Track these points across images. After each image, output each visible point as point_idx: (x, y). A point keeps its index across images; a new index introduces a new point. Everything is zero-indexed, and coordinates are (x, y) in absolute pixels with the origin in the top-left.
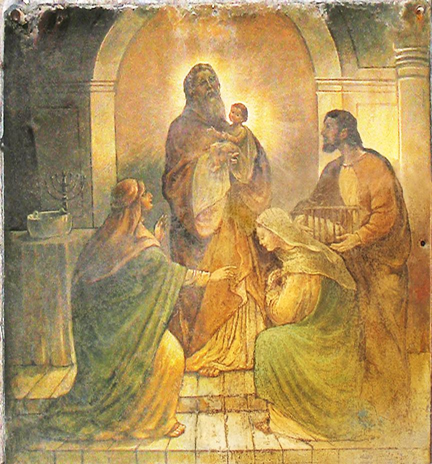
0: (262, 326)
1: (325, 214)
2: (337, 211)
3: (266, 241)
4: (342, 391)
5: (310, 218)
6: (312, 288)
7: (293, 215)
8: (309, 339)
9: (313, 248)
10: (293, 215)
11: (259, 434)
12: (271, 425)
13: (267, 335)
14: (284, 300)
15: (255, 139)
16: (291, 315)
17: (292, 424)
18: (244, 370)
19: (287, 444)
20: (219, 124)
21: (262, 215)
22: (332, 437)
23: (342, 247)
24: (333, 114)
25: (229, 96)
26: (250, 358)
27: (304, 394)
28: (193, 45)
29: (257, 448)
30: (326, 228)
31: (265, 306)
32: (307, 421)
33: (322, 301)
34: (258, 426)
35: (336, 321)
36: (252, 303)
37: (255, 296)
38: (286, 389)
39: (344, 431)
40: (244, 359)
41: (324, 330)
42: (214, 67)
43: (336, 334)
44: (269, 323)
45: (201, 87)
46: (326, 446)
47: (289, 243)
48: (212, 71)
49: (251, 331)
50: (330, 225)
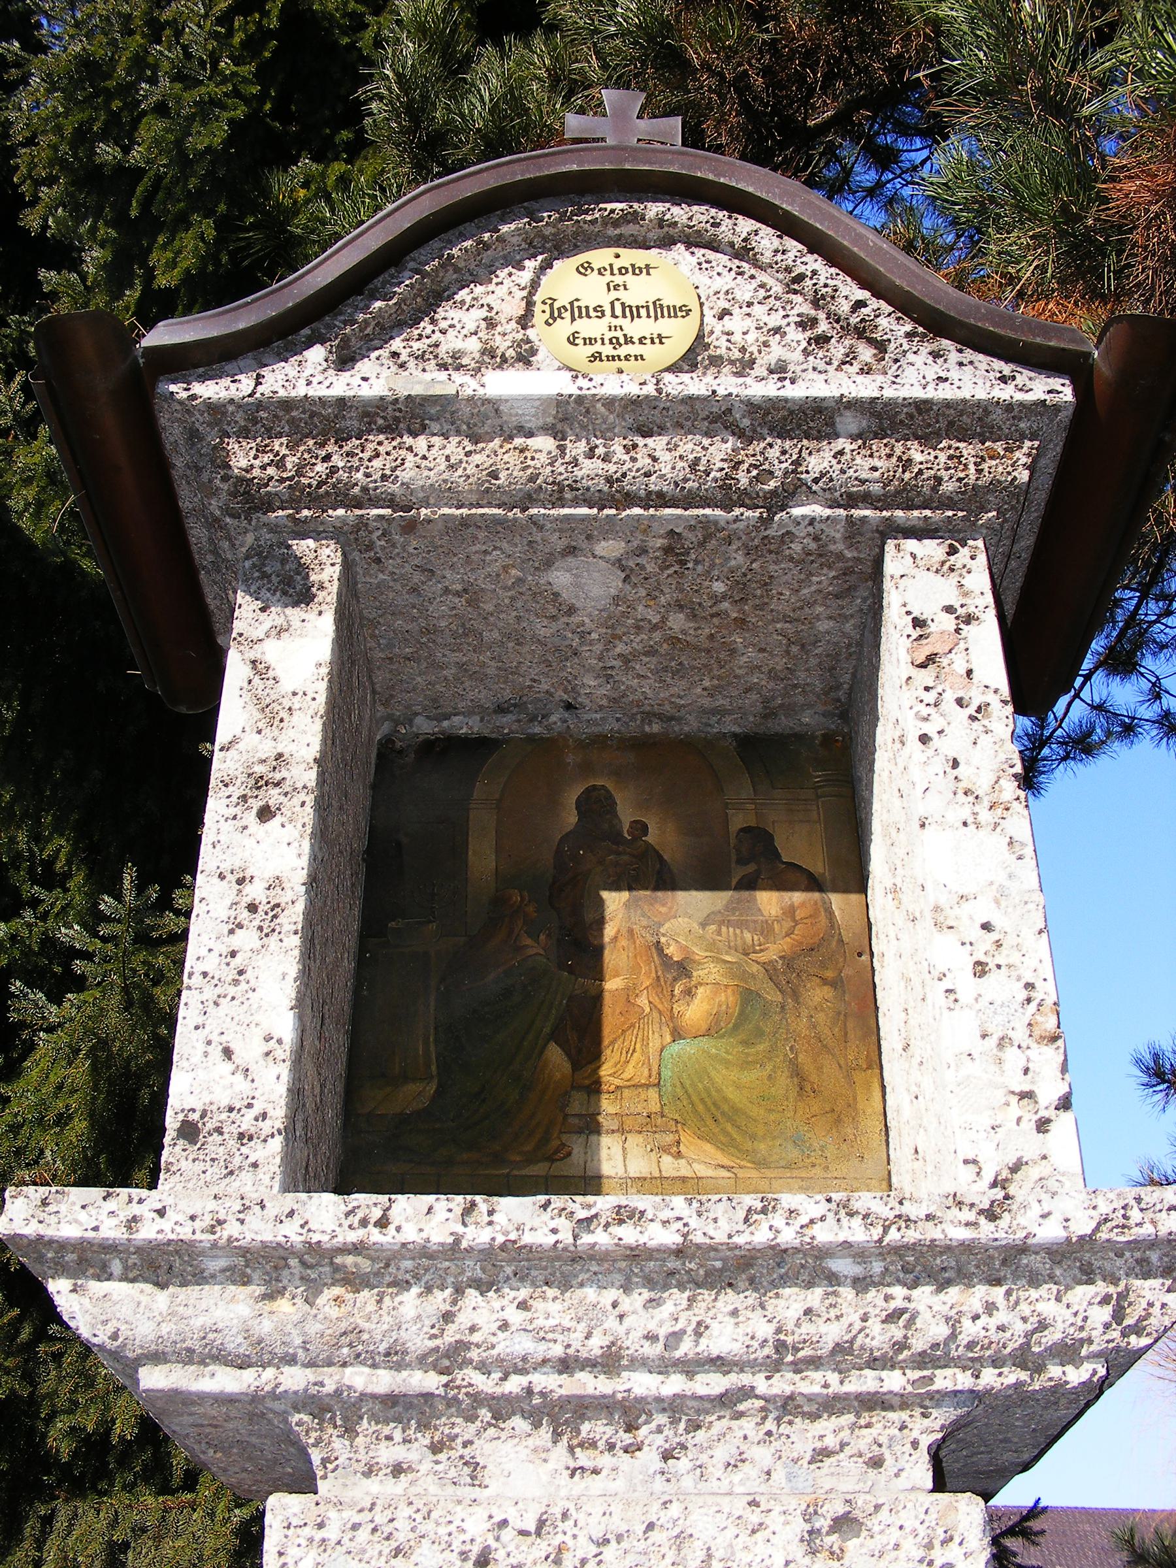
0: (668, 1038)
1: (741, 925)
2: (755, 922)
3: (672, 950)
4: (771, 1111)
5: (724, 929)
6: (728, 998)
7: (703, 925)
8: (727, 1052)
9: (728, 958)
10: (703, 925)
11: (667, 1160)
12: (682, 1148)
13: (676, 1048)
14: (695, 1011)
15: (657, 852)
16: (704, 1027)
17: (708, 1147)
18: (647, 1086)
19: (702, 1170)
20: (617, 838)
21: (667, 925)
22: (761, 1164)
23: (763, 957)
24: (746, 830)
25: (626, 815)
26: (654, 1073)
27: (723, 1114)
28: (587, 769)
29: (665, 1174)
30: (742, 938)
31: (672, 1017)
32: (727, 1145)
33: (742, 1013)
34: (664, 1149)
35: (759, 1033)
36: (655, 1014)
37: (660, 1006)
38: (701, 1108)
39: (775, 1157)
40: (646, 1072)
41: (745, 1043)
42: (610, 786)
43: (761, 1047)
44: (677, 1035)
45: (596, 806)
46: (754, 1174)
47: (699, 953)
48: (608, 791)
49: (654, 1043)
50: (748, 936)
